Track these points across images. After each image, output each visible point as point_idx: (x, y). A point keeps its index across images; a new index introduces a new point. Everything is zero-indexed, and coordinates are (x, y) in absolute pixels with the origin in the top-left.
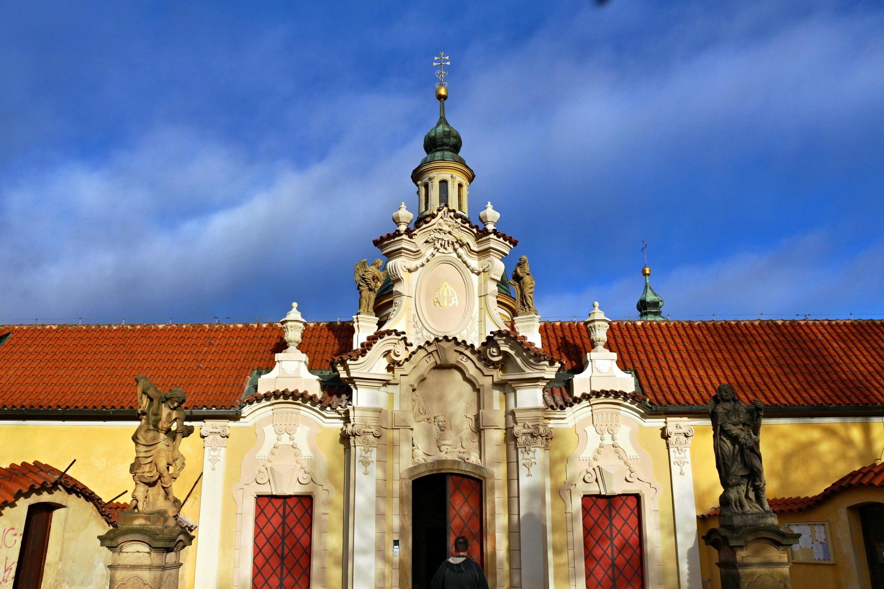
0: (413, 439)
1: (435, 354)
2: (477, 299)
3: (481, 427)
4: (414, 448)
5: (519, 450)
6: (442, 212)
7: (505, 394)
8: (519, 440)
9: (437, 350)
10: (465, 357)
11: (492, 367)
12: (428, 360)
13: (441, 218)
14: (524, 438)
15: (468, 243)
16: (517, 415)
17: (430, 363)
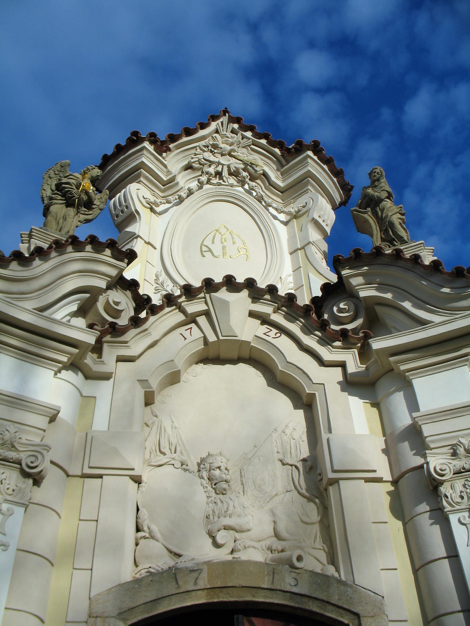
0: (138, 510)
1: (202, 320)
2: (288, 259)
3: (332, 475)
5: (453, 519)
6: (219, 121)
7: (376, 405)
8: (444, 489)
9: (207, 314)
10: (274, 331)
11: (338, 344)
12: (187, 334)
13: (217, 132)
14: (459, 485)
15: (265, 174)
16: (427, 430)
17: (189, 339)
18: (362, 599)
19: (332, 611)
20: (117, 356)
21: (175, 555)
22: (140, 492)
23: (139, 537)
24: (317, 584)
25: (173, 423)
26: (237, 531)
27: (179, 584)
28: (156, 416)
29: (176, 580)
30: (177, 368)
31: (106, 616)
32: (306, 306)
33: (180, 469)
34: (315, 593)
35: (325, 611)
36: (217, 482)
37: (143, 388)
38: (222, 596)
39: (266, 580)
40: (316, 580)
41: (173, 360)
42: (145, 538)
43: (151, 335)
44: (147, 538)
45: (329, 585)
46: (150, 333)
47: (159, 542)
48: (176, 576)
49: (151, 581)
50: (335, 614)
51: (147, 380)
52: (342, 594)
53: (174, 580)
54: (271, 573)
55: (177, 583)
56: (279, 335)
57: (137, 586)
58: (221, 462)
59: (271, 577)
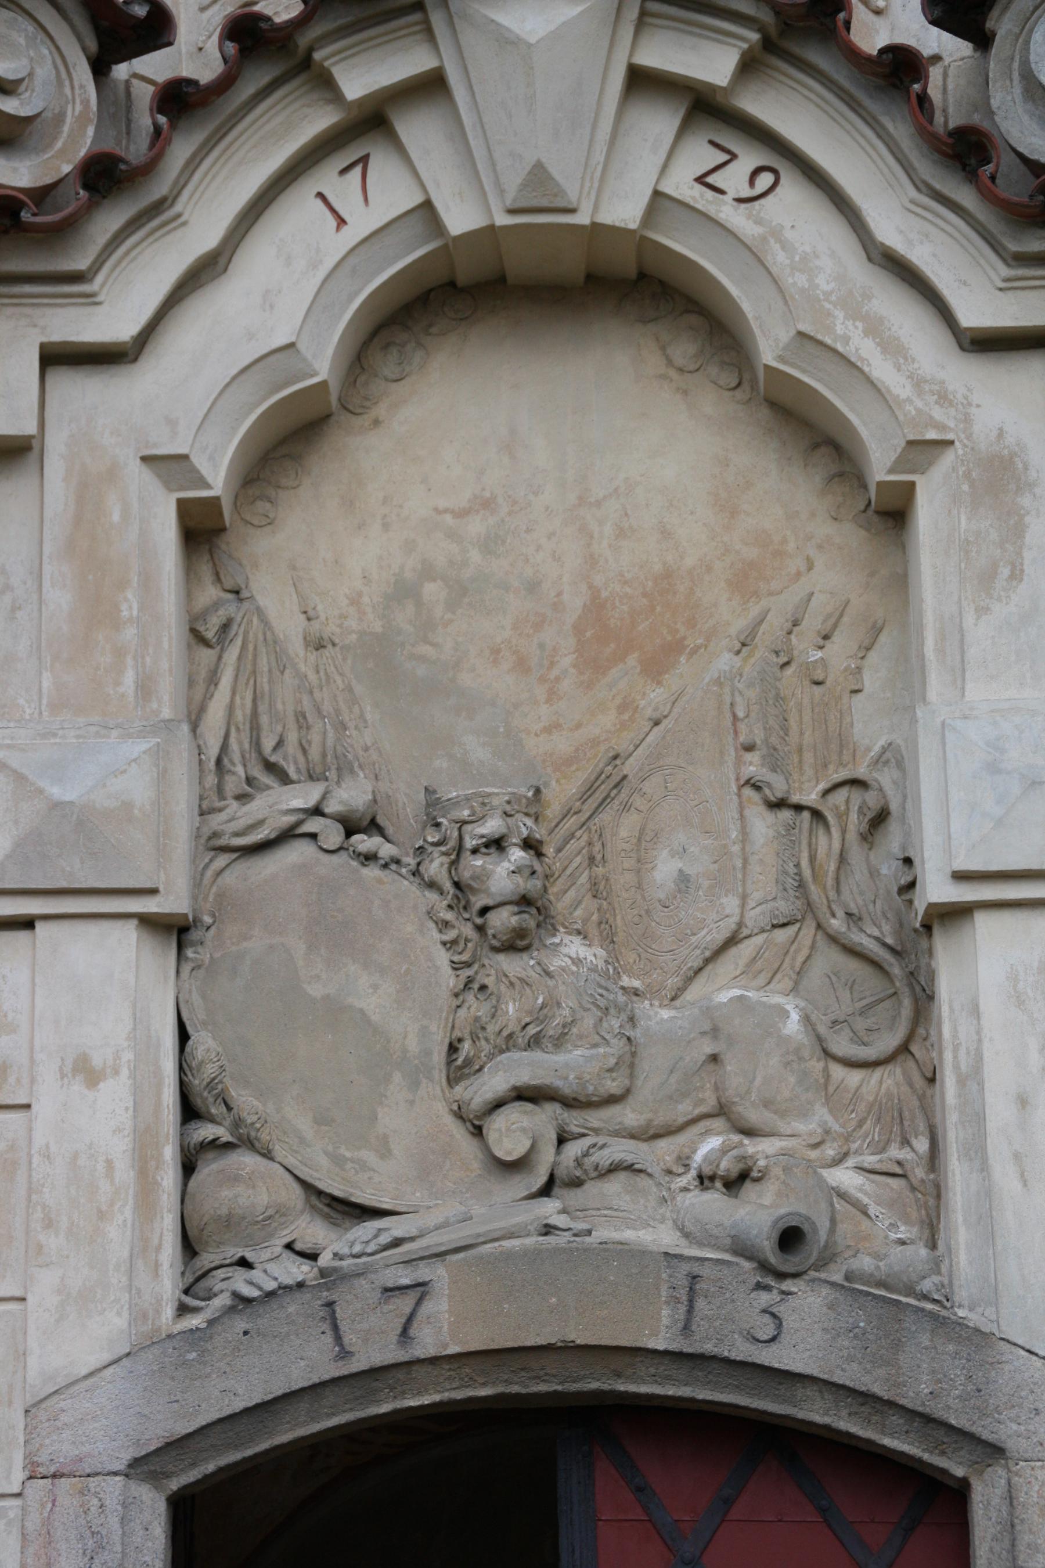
0: (183, 1036)
4: (206, 1132)
18: (1023, 1394)
19: (907, 1432)
20: (42, 346)
21: (334, 1204)
22: (186, 968)
23: (192, 1145)
24: (856, 1337)
25: (309, 619)
26: (570, 1103)
27: (346, 1340)
28: (237, 592)
29: (335, 1328)
30: (312, 376)
31: (88, 1471)
32: (890, 56)
33: (342, 858)
34: (843, 1370)
35: (883, 1433)
36: (490, 902)
37: (169, 488)
38: (506, 1377)
39: (665, 1321)
40: (851, 1320)
41: (292, 345)
42: (214, 1145)
43: (184, 224)
44: (228, 1146)
45: (899, 1340)
46: (179, 216)
47: (272, 1159)
48: (334, 1312)
49: (246, 1333)
50: (917, 1444)
51: (186, 457)
52: (945, 1376)
53: (326, 1326)
54: (683, 1294)
55: (338, 1338)
56: (765, 180)
57: (193, 1355)
58: (505, 813)
59: (683, 1309)
